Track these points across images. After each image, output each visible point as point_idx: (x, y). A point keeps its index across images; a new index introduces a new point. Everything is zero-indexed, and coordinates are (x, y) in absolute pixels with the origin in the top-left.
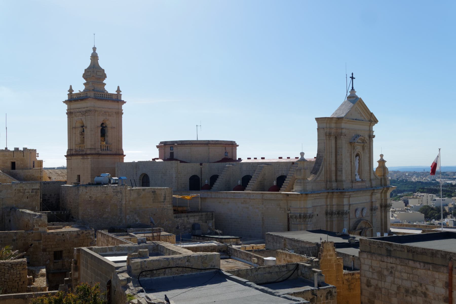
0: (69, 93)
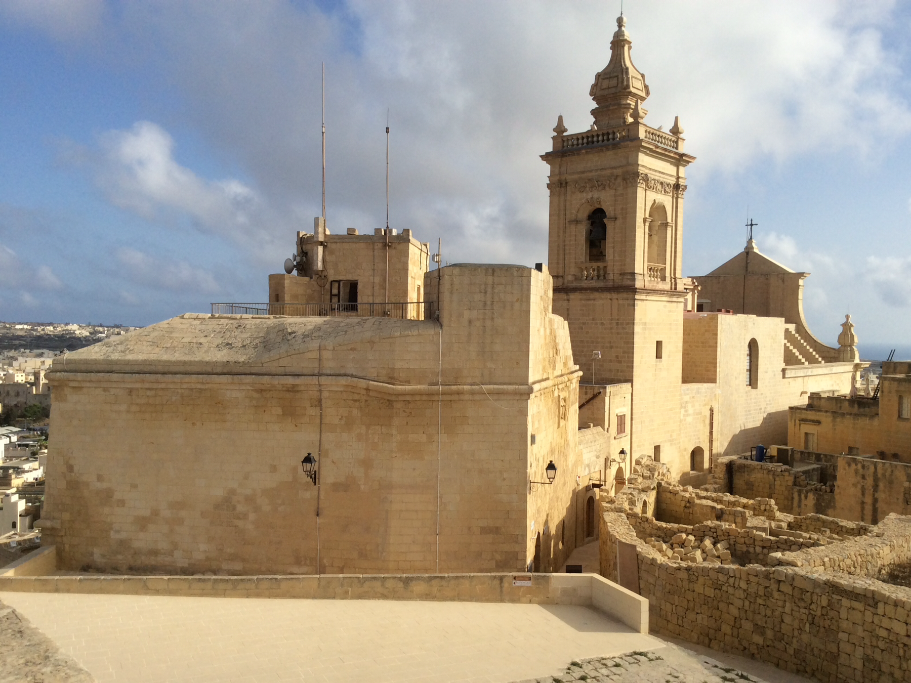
0: (555, 134)
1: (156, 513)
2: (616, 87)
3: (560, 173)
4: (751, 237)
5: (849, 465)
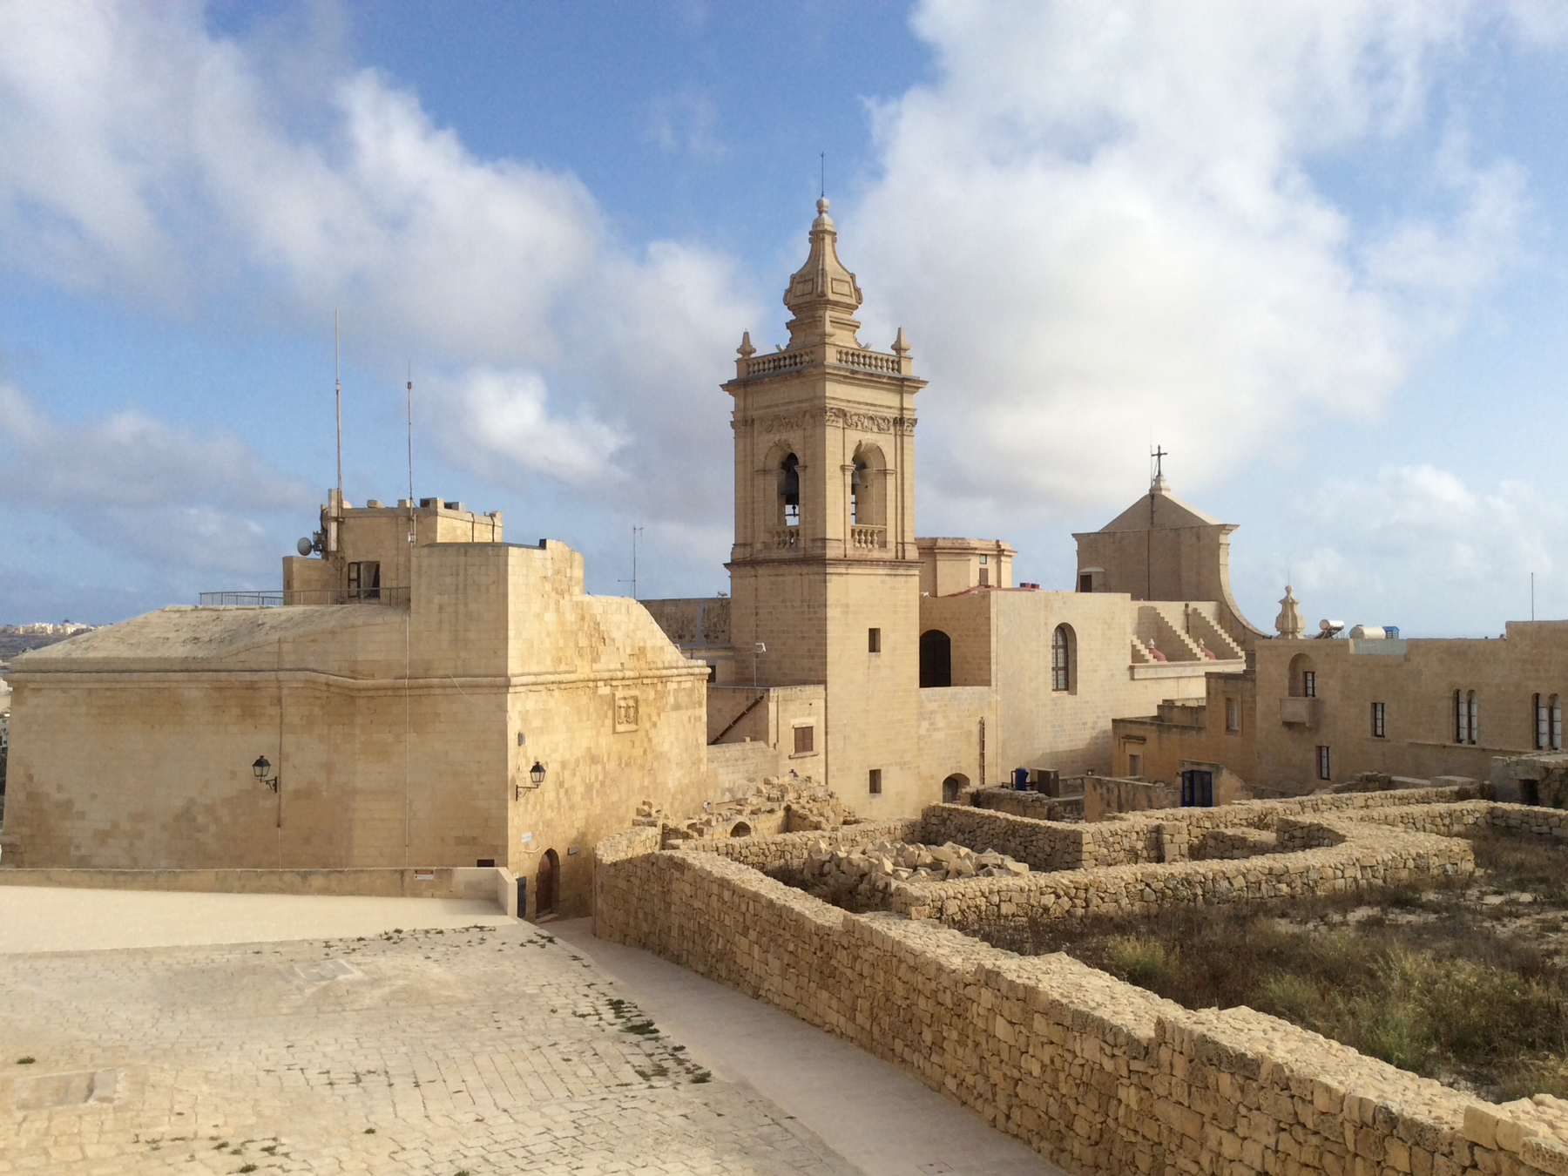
0: (740, 356)
1: (115, 826)
2: (811, 293)
3: (745, 409)
4: (1159, 472)
5: (1095, 789)
